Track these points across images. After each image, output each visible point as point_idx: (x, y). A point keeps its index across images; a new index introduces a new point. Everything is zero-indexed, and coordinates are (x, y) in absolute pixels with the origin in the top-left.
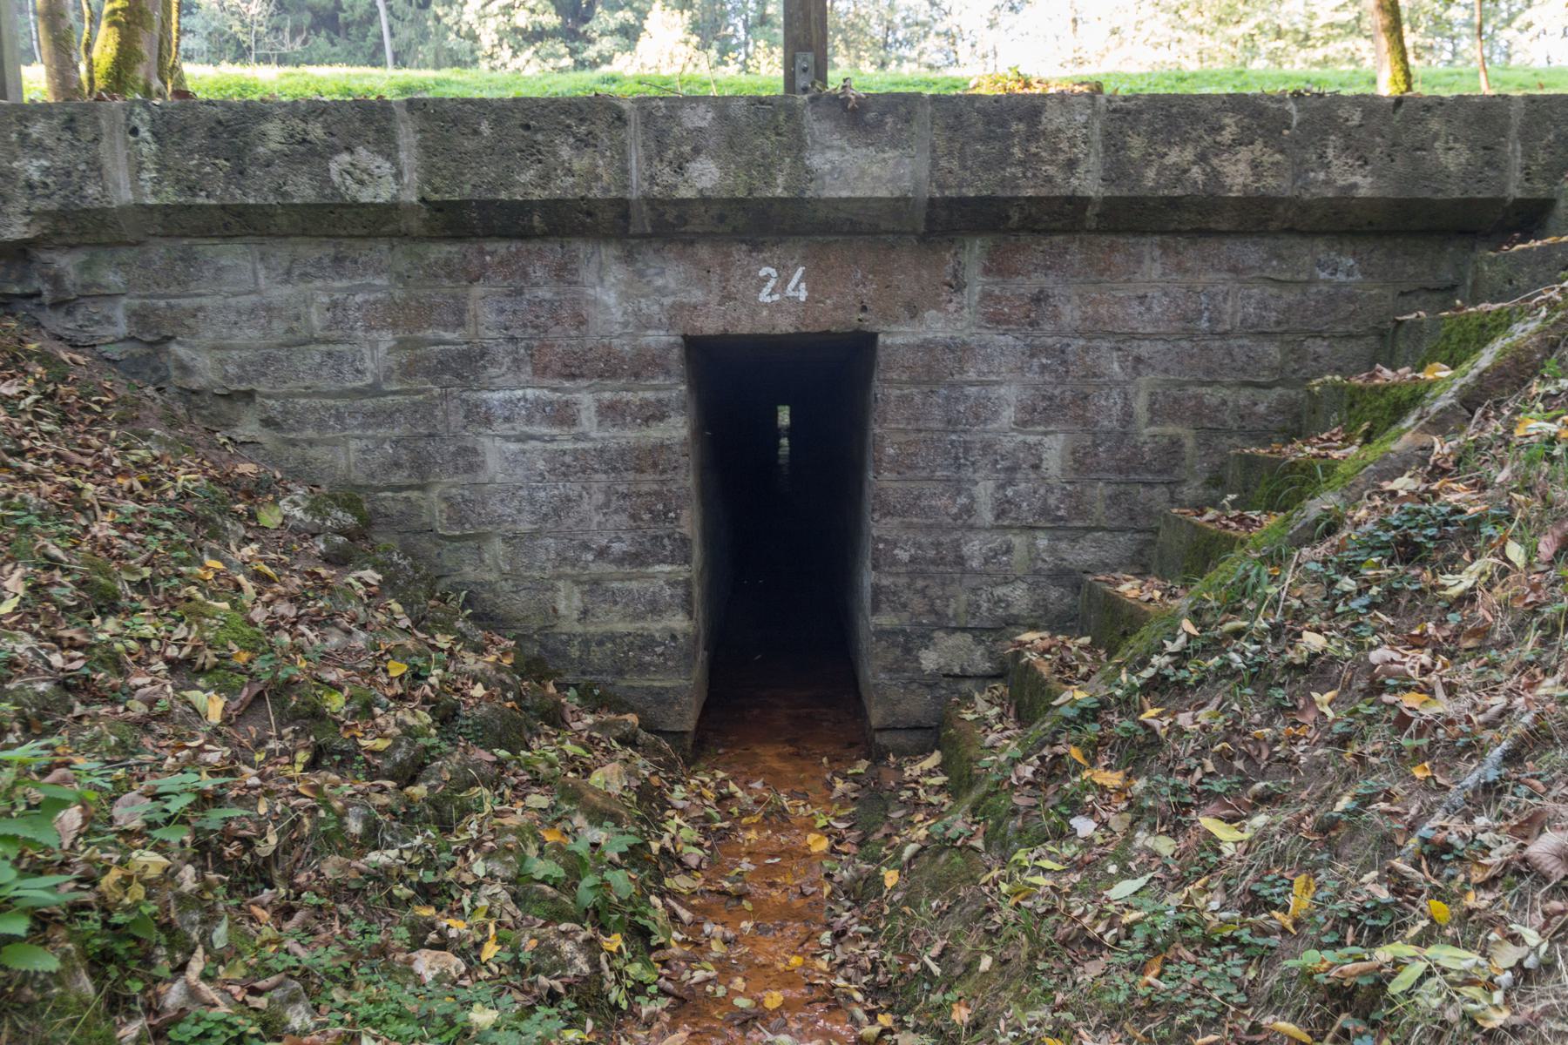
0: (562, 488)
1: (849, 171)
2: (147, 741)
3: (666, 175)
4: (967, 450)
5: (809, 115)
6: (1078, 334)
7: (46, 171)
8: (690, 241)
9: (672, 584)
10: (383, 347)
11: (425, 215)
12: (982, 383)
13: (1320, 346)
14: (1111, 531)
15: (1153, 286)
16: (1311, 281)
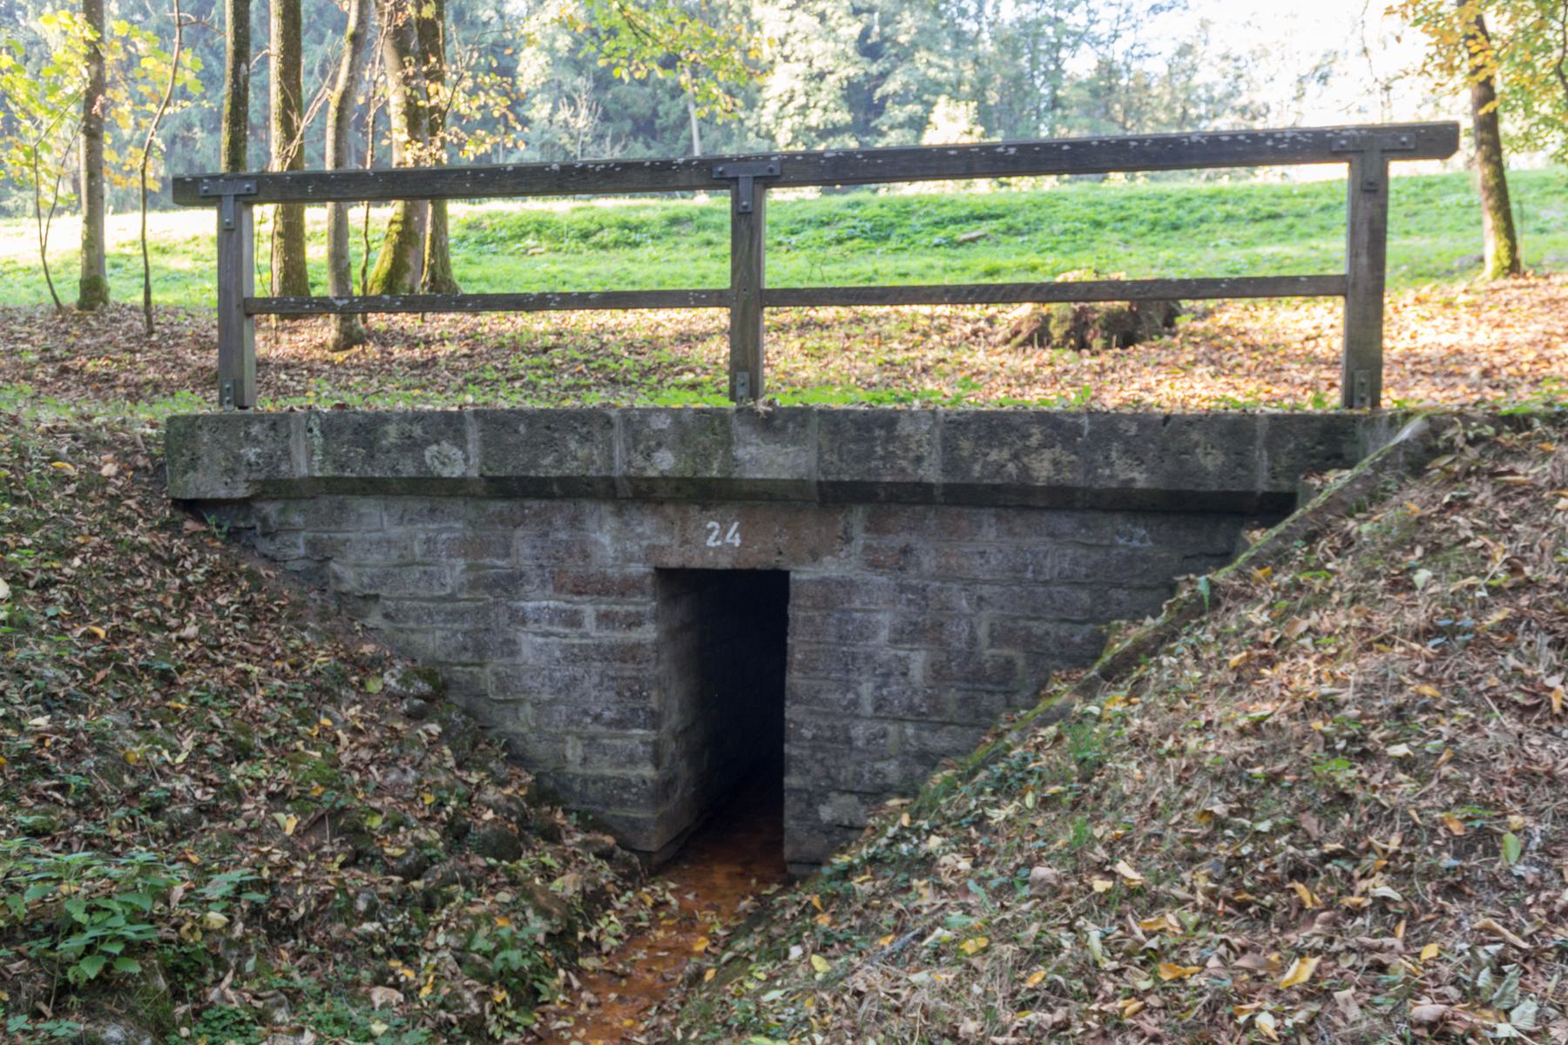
0: (571, 670)
1: (763, 460)
2: (241, 846)
3: (639, 460)
4: (854, 659)
5: (735, 421)
6: (934, 577)
7: (259, 455)
8: (661, 503)
9: (644, 743)
10: (458, 569)
11: (484, 484)
12: (864, 611)
13: (1121, 595)
14: (962, 725)
15: (989, 545)
16: (1113, 545)
